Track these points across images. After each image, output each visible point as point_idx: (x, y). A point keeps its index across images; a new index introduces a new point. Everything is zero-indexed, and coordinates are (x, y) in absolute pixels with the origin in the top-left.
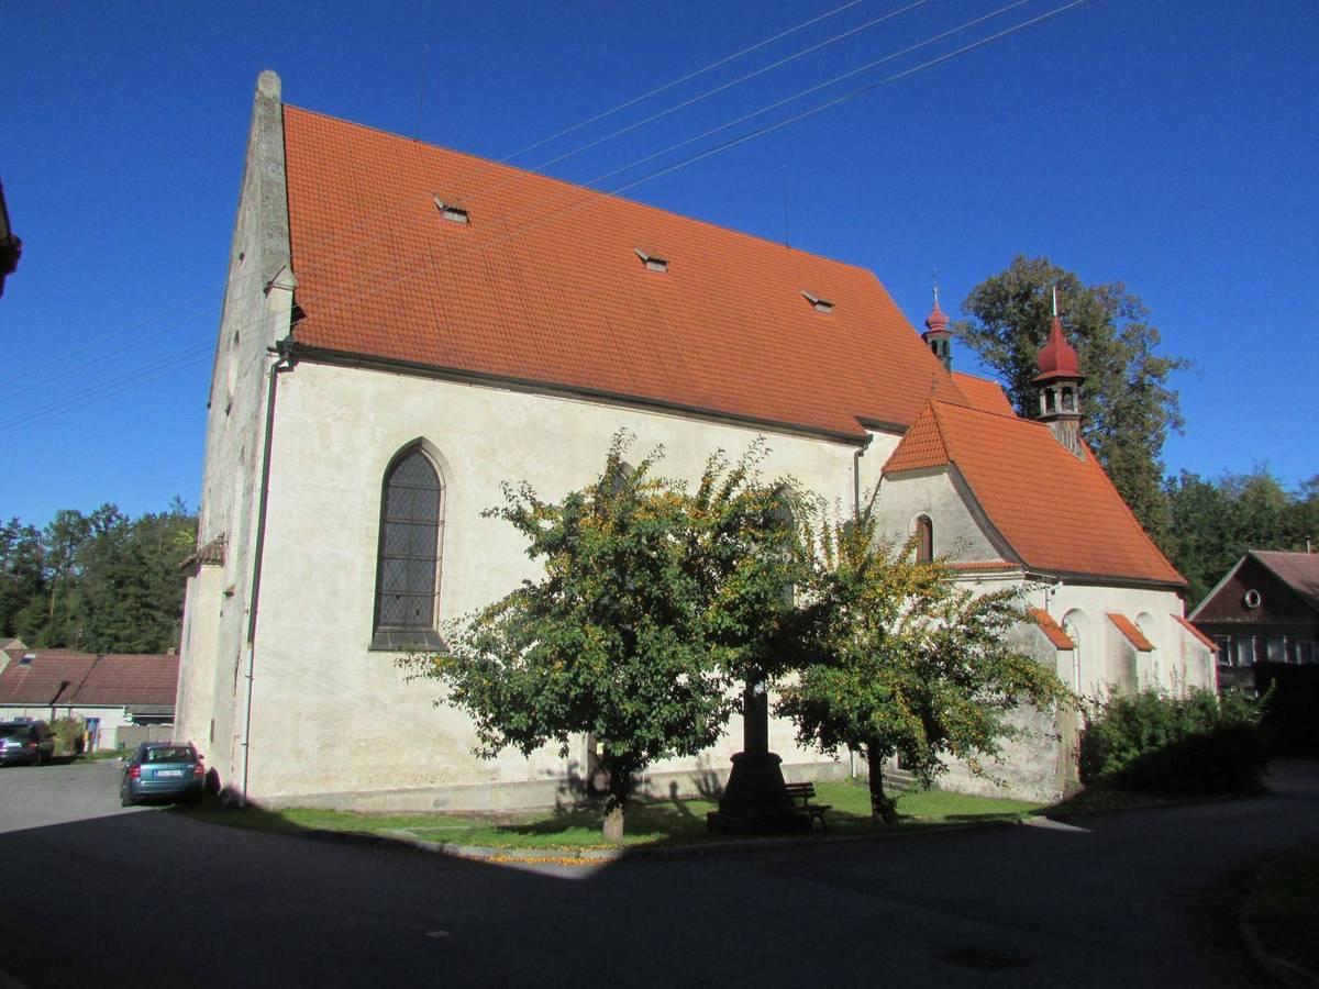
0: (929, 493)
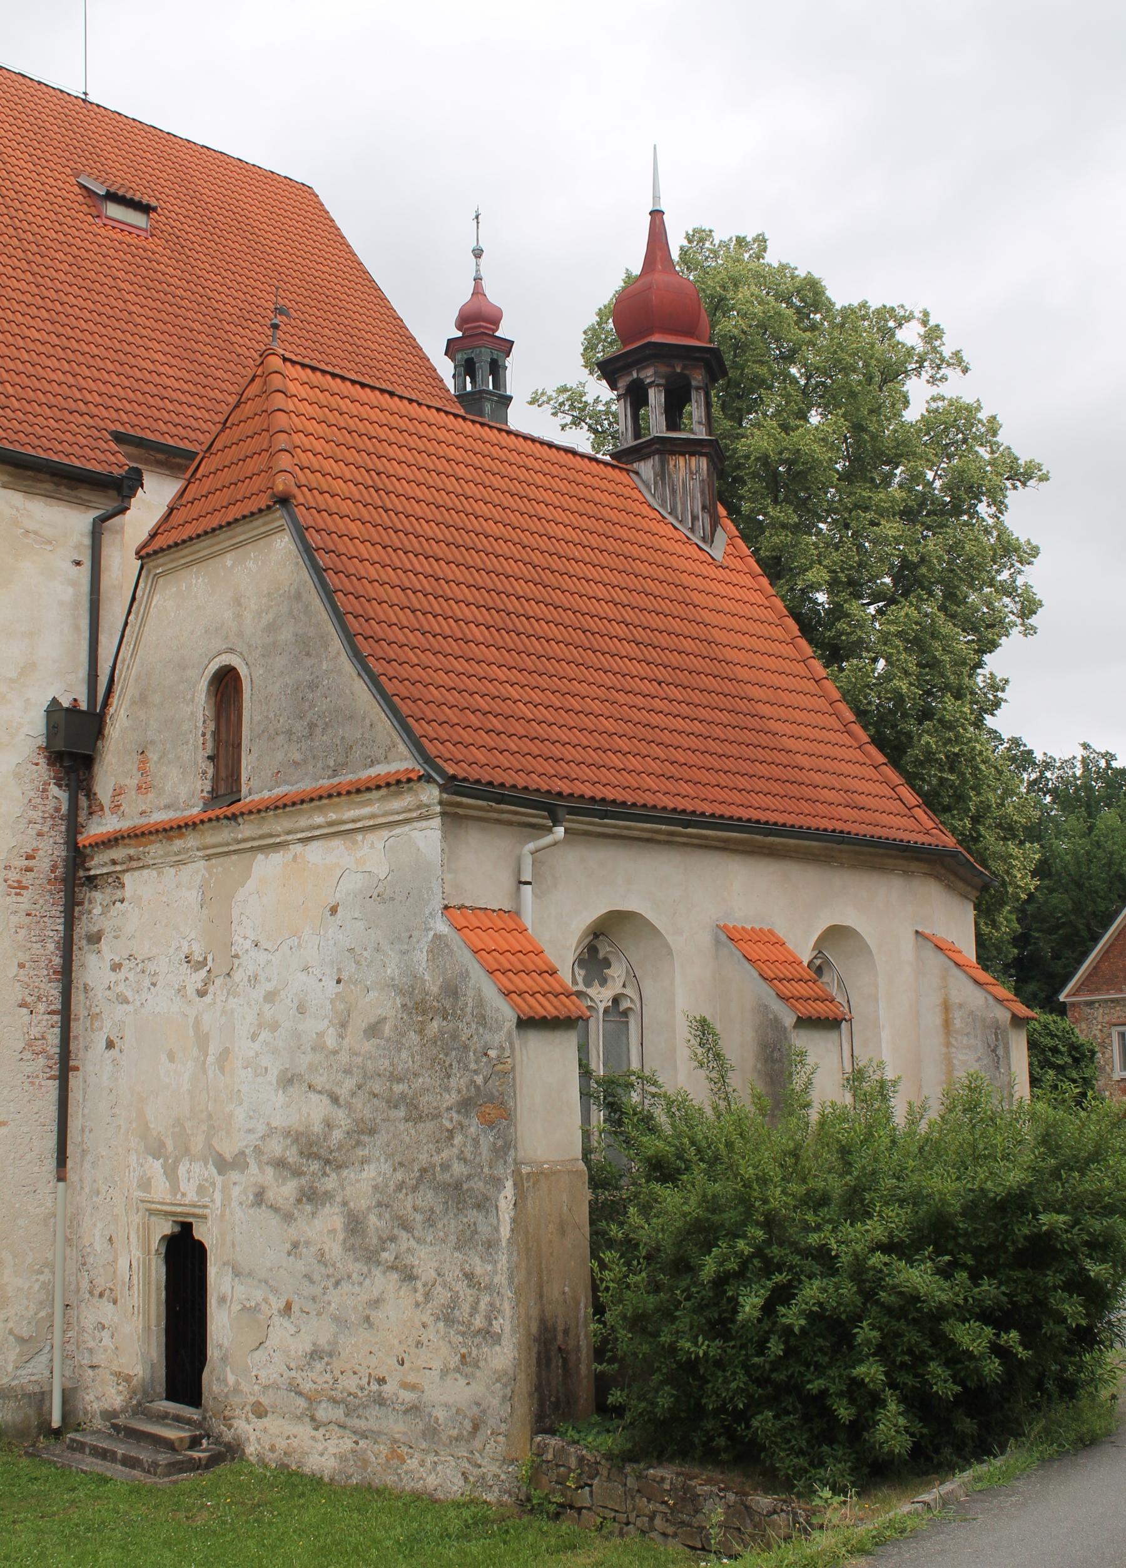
0: (237, 602)
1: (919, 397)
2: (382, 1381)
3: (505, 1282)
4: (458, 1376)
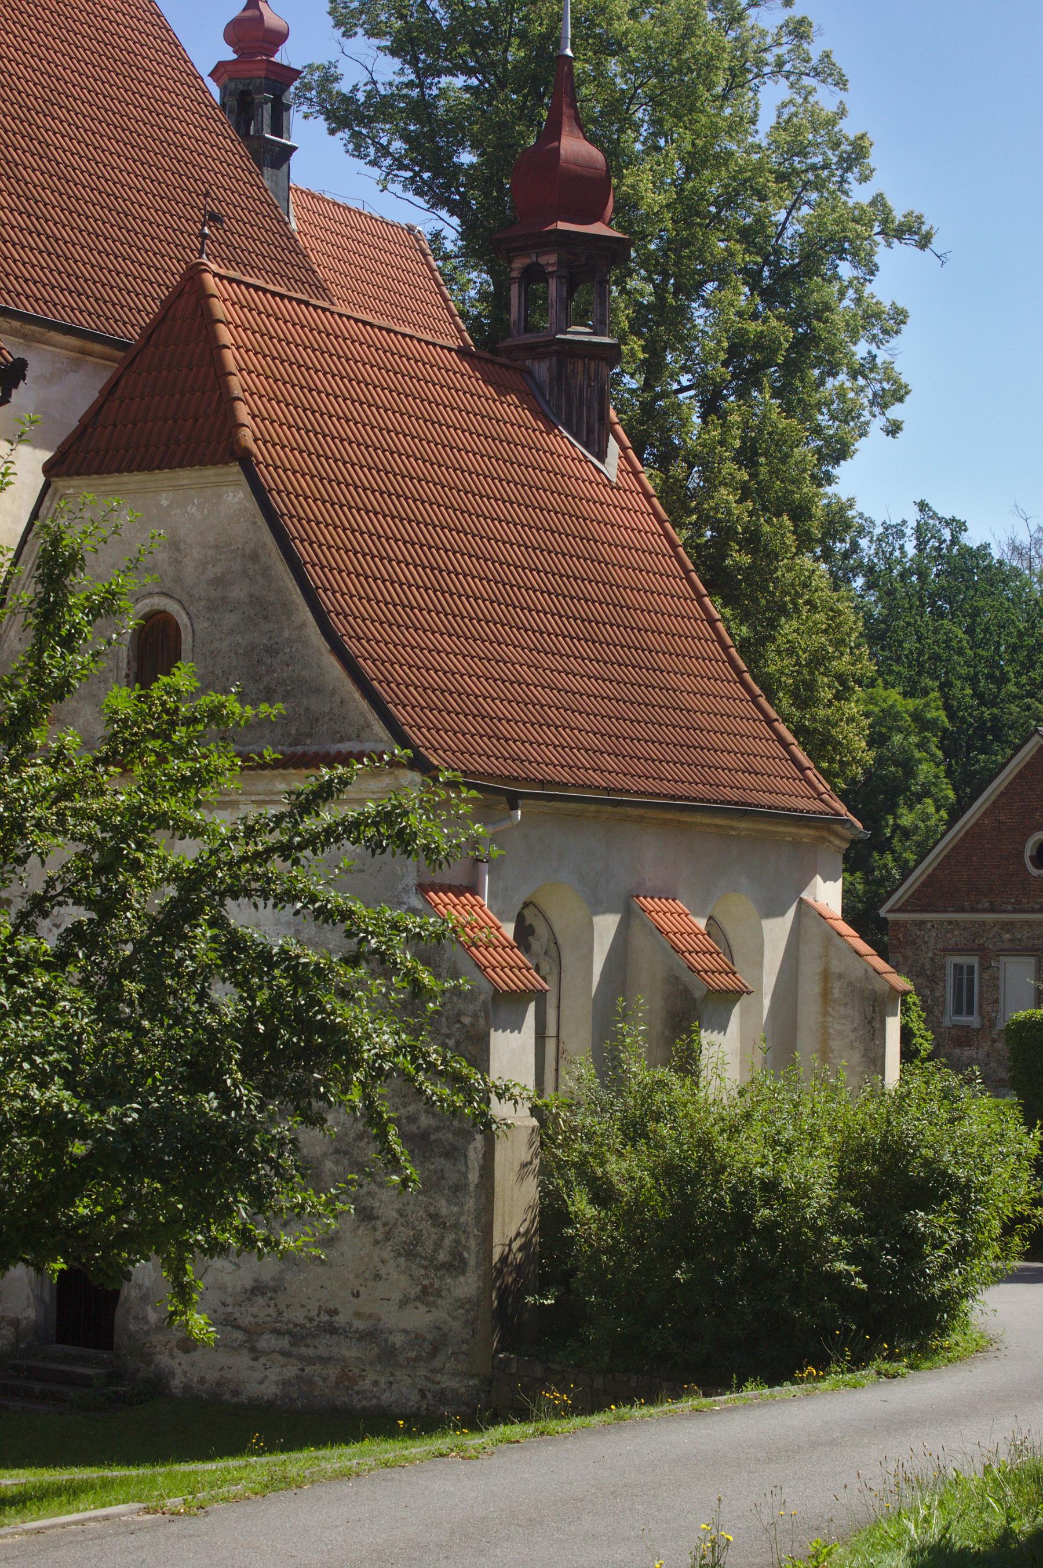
1: (771, 98)
2: (333, 1312)
3: (471, 1220)
4: (418, 1304)
